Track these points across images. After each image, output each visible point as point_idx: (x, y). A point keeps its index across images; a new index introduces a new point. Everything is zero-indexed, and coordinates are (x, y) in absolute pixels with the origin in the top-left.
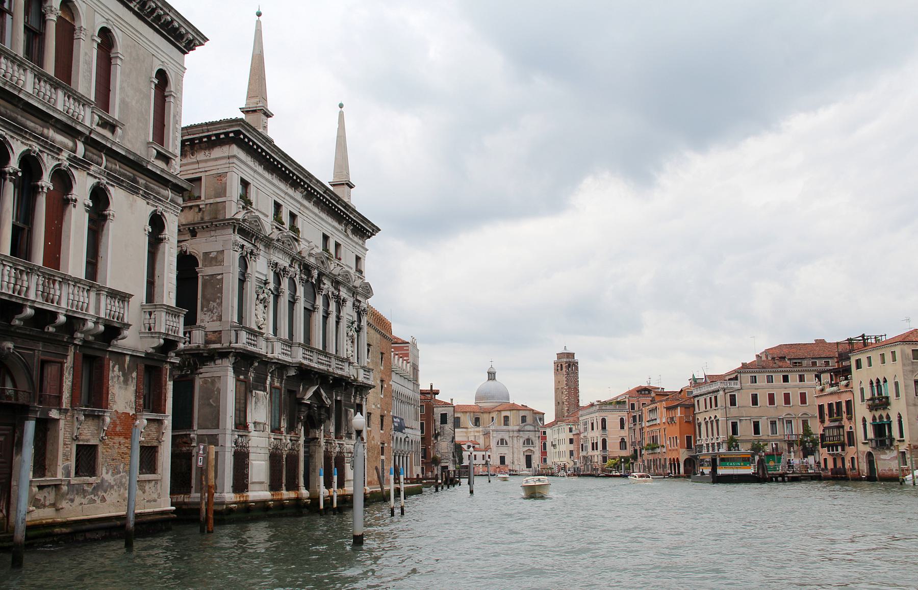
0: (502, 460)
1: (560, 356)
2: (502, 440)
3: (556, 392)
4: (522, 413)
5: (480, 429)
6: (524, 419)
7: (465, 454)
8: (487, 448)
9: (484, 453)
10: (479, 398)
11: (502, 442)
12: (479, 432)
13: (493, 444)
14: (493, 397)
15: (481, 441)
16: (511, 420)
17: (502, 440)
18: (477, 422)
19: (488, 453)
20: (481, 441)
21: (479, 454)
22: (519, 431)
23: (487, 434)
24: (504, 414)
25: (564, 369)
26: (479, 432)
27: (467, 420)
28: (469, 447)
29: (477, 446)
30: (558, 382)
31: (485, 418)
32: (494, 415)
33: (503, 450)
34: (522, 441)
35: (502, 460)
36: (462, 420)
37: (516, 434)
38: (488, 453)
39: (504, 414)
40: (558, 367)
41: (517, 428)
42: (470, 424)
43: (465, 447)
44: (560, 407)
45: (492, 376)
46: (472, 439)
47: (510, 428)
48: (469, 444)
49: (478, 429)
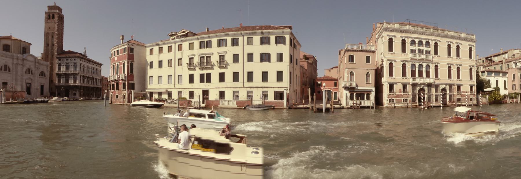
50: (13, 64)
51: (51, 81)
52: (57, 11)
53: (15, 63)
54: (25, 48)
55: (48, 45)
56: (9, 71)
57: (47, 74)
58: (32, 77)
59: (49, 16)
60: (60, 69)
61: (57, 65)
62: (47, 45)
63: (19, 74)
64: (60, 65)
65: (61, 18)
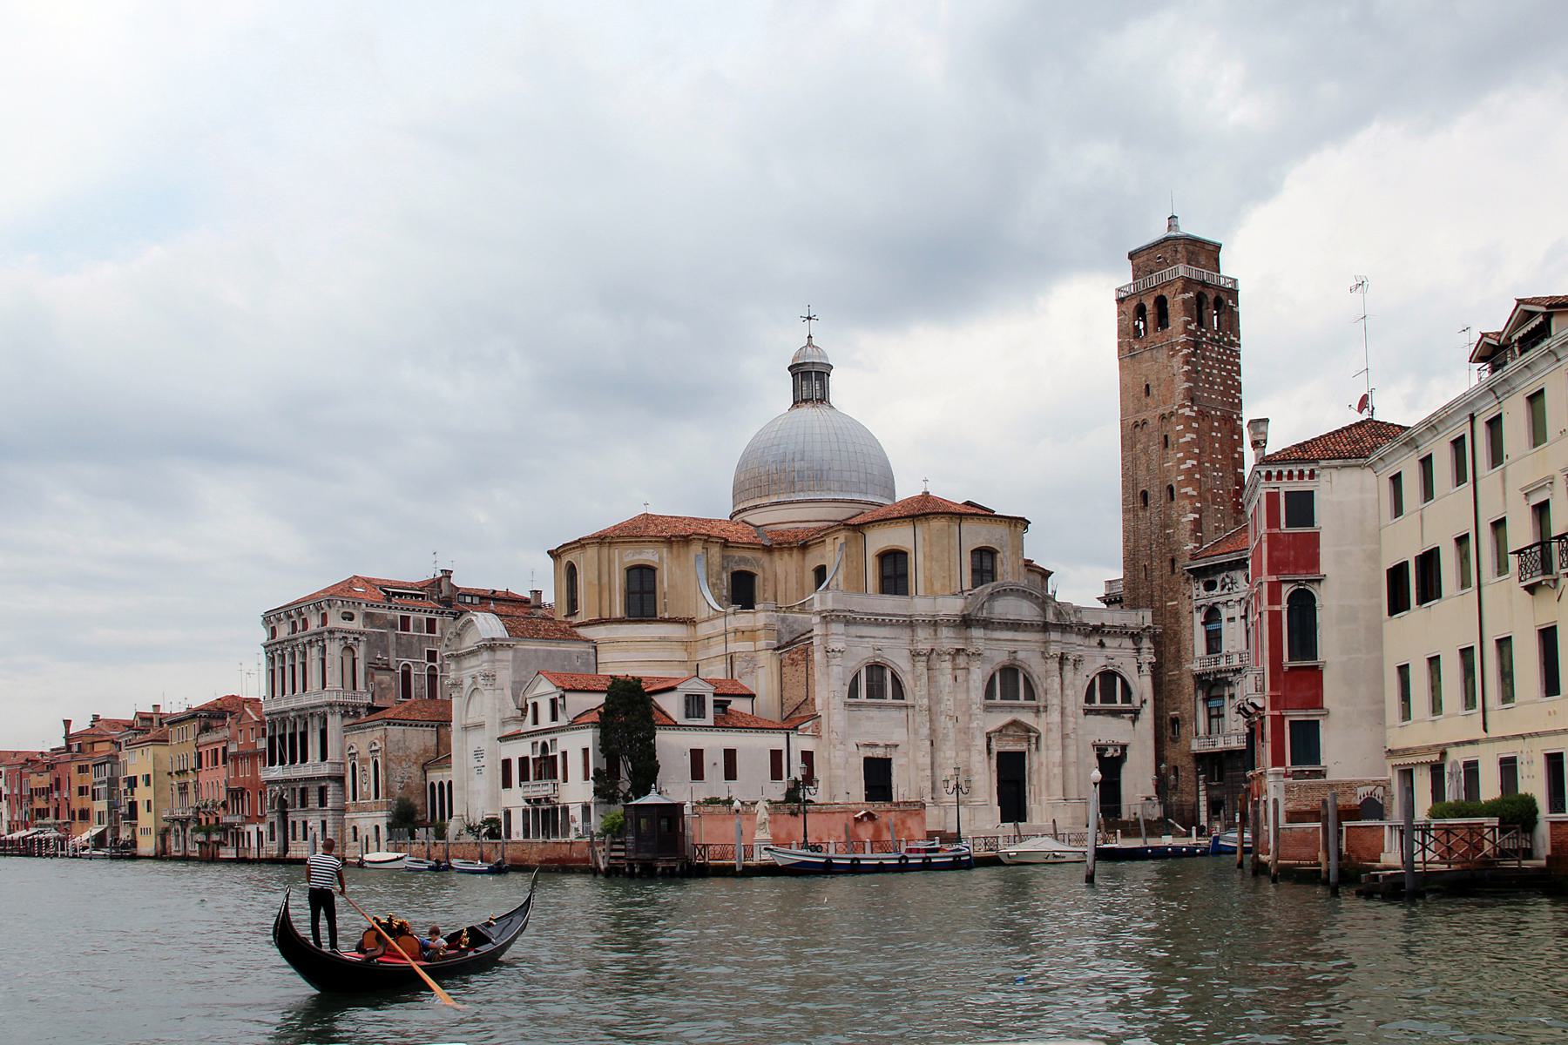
0: (878, 776)
1: (1145, 259)
2: (876, 669)
3: (1128, 442)
4: (976, 535)
5: (759, 617)
6: (984, 563)
7: (672, 746)
8: (796, 716)
9: (777, 741)
10: (756, 481)
11: (877, 683)
12: (749, 634)
13: (828, 689)
14: (818, 477)
15: (764, 681)
16: (919, 570)
17: (876, 669)
18: (742, 591)
19: (801, 743)
20: (764, 681)
21: (754, 747)
22: (966, 622)
23: (793, 648)
24: (880, 539)
25: (1177, 319)
26: (749, 634)
27: (690, 582)
28: (694, 704)
29: (738, 705)
30: (1137, 393)
31: (781, 572)
32: (830, 554)
33: (883, 727)
34: (978, 676)
35: (878, 776)
36: (664, 581)
37: (948, 639)
38: (801, 743)
39: (880, 539)
40: (1143, 315)
41: (953, 606)
42: (707, 601)
43: (672, 705)
44: (1153, 514)
45: (810, 379)
46: (718, 671)
47: (919, 605)
48: (695, 687)
49: (744, 620)
50: (915, 654)
51: (1167, 730)
52: (1182, 270)
53: (924, 646)
54: (990, 549)
55: (1145, 495)
56: (899, 692)
57: (1142, 686)
58: (1027, 718)
59: (1140, 311)
60: (1214, 641)
61: (1199, 618)
62: (1138, 499)
63: (948, 704)
64: (1212, 614)
65: (1215, 307)
